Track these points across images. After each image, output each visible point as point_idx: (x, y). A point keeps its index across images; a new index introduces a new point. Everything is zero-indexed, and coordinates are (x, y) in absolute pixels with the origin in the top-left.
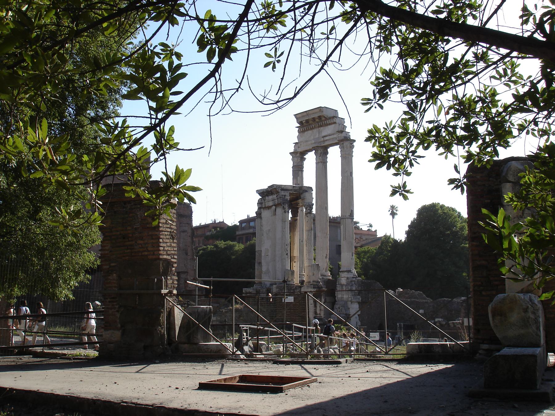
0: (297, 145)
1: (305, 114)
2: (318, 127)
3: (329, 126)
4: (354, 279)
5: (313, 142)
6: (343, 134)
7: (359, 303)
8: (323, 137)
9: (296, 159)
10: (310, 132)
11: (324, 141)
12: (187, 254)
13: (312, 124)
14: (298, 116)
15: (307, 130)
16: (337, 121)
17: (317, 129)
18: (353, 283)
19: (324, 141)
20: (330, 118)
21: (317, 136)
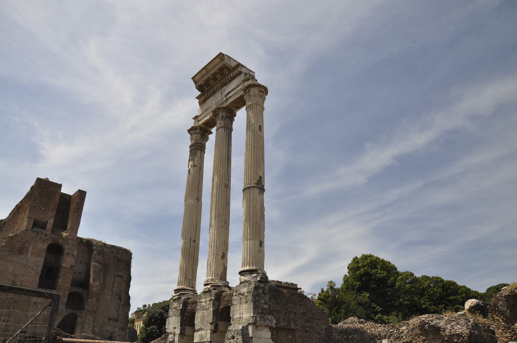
0: (197, 120)
1: (204, 72)
2: (221, 87)
3: (233, 81)
4: (262, 285)
5: (215, 106)
6: (250, 82)
7: (271, 329)
8: (226, 96)
9: (194, 136)
10: (212, 98)
11: (227, 100)
12: (120, 299)
13: (213, 87)
14: (196, 79)
15: (209, 98)
16: (243, 70)
17: (220, 91)
18: (260, 291)
19: (227, 100)
20: (235, 68)
21: (219, 98)
